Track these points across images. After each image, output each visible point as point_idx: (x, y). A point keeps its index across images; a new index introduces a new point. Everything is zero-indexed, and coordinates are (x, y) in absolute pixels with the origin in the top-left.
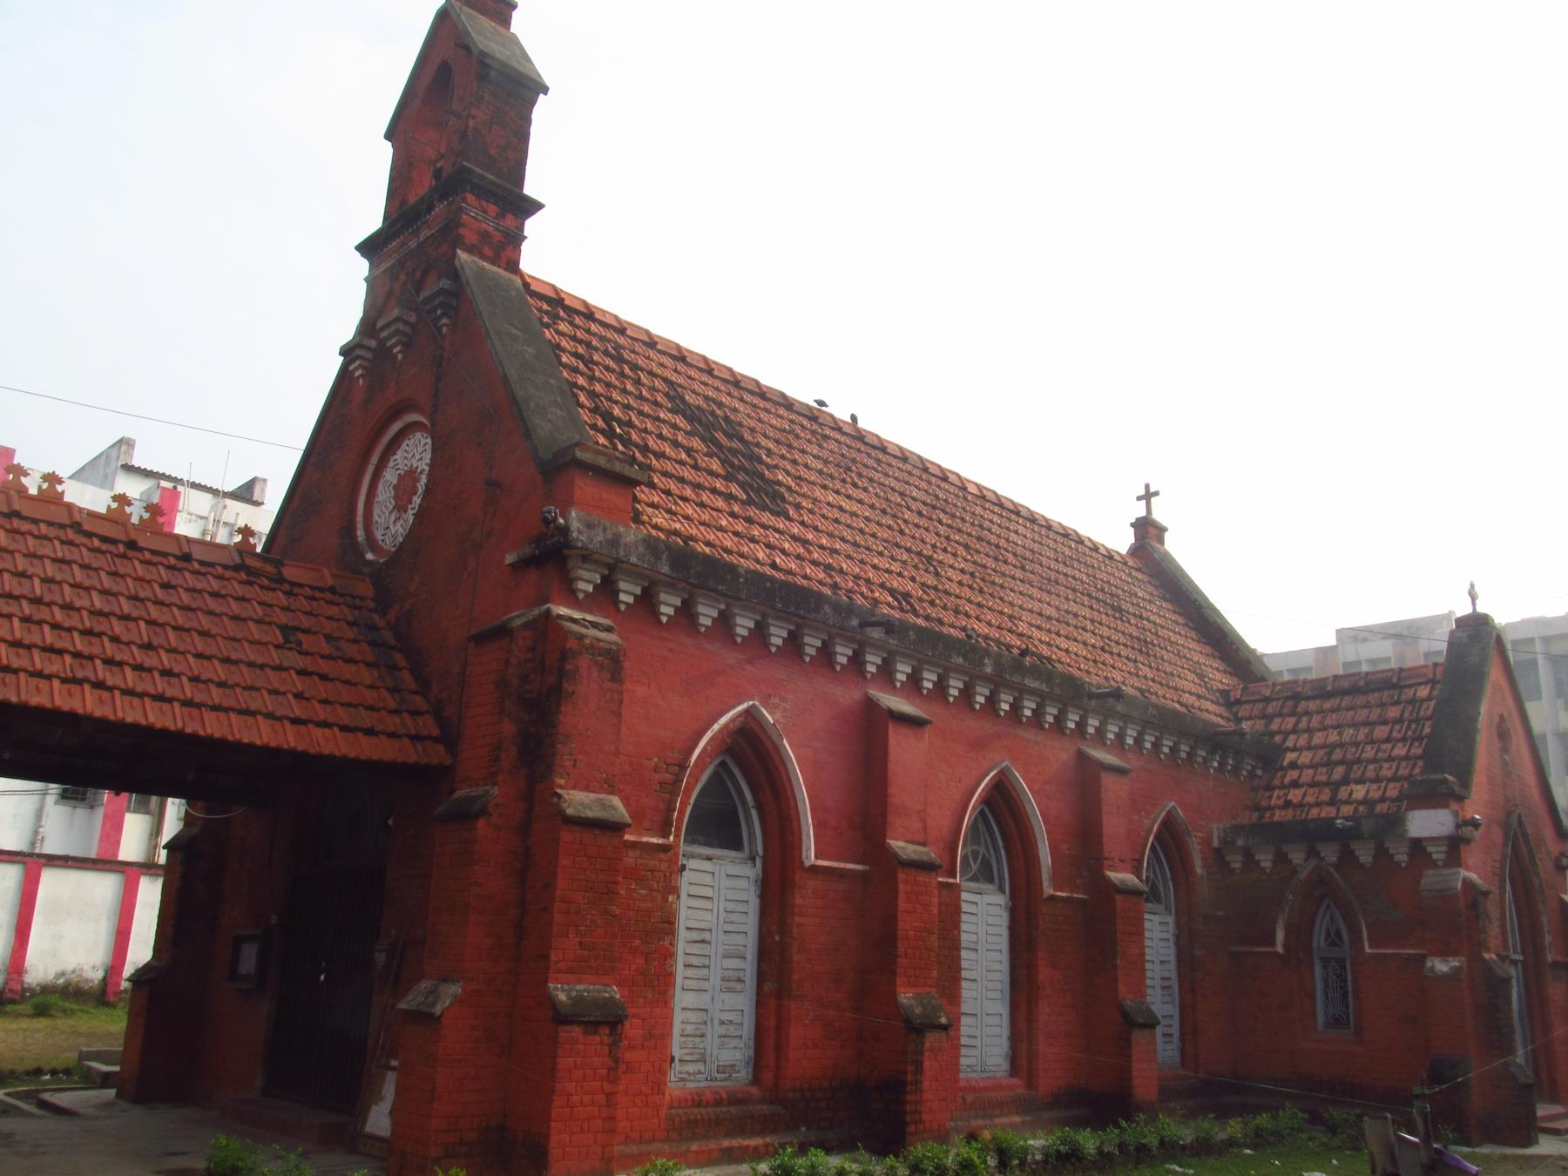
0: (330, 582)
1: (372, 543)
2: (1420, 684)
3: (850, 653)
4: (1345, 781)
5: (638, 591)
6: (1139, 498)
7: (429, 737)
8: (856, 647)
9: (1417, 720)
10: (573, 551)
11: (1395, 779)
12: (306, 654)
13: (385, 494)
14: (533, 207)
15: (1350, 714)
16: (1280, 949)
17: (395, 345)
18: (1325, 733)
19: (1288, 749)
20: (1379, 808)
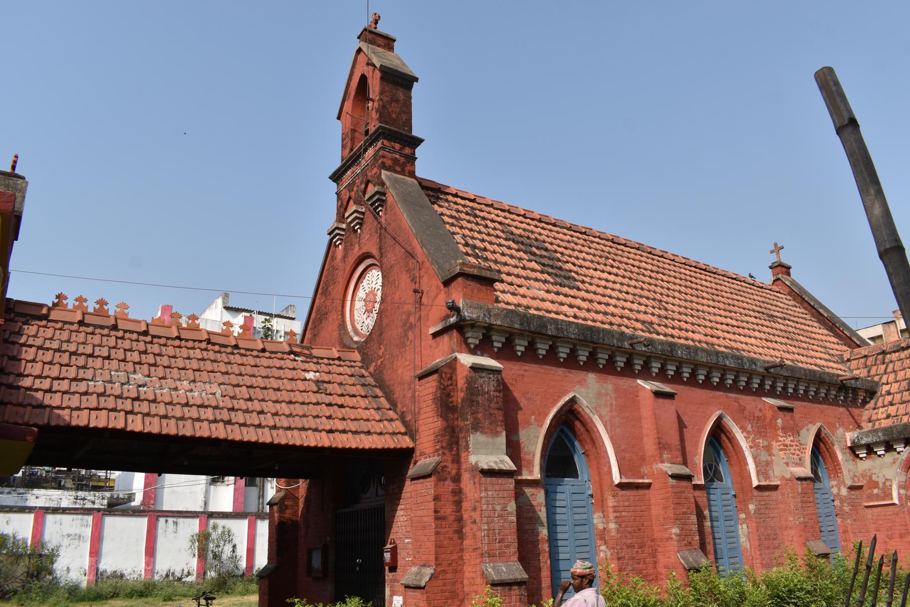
0: (337, 355)
1: (356, 332)
3: (625, 360)
5: (503, 340)
6: (772, 252)
7: (400, 433)
12: (330, 394)
13: (359, 305)
14: (418, 142)
16: (896, 501)
17: (356, 225)
18: (904, 372)
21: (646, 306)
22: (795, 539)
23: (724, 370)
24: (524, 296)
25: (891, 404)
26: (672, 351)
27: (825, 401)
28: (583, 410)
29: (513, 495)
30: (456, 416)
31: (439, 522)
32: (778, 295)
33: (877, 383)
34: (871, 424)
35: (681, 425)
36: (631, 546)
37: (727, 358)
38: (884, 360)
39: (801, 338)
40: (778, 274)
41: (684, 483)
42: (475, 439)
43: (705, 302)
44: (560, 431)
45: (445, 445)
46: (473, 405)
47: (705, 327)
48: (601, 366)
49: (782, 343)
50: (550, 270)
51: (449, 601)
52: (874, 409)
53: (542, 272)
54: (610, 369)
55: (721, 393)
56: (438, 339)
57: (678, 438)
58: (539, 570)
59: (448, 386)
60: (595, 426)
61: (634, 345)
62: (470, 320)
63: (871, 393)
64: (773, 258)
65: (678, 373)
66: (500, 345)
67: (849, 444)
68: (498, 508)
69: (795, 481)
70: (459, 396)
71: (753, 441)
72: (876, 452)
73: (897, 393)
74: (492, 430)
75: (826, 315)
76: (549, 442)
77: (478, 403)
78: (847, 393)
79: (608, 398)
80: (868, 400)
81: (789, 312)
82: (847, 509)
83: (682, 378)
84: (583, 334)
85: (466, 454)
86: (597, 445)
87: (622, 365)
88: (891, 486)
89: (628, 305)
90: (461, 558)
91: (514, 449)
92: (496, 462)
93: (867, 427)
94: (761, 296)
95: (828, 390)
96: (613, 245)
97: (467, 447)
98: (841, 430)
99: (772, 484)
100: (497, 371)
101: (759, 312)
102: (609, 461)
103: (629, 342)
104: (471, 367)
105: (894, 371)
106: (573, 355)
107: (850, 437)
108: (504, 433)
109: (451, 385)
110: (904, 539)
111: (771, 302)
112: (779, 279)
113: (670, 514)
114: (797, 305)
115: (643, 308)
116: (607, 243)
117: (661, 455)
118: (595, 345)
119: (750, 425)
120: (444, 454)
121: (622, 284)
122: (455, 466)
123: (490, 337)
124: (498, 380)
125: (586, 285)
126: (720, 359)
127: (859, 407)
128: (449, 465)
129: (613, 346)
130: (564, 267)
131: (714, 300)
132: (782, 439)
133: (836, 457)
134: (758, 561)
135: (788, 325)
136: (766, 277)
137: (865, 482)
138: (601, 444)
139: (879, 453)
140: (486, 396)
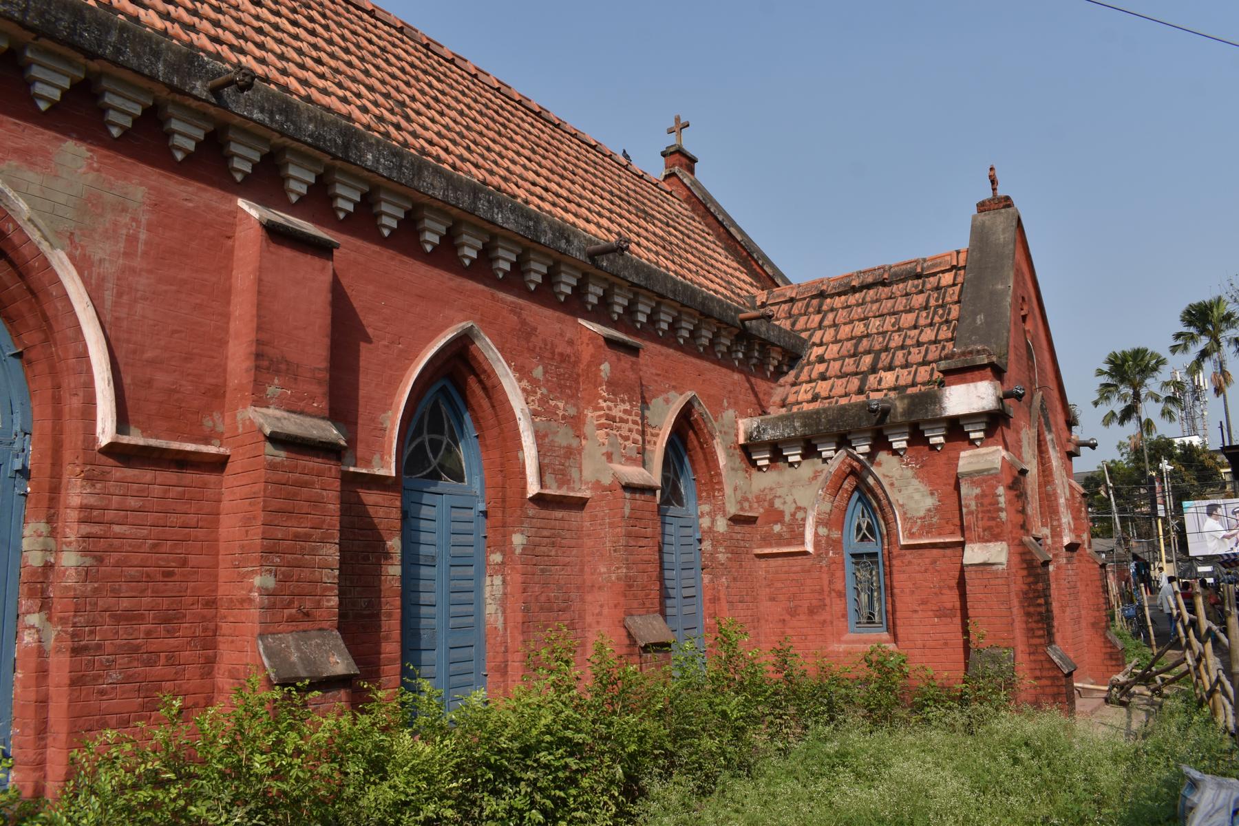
2: (943, 272)
4: (874, 369)
6: (670, 131)
9: (942, 306)
11: (924, 363)
15: (875, 306)
16: (809, 548)
18: (850, 326)
19: (814, 344)
22: (606, 611)
25: (823, 377)
26: (346, 147)
27: (708, 354)
28: (18, 228)
32: (668, 196)
33: (804, 342)
36: (131, 617)
38: (820, 306)
40: (674, 165)
52: (794, 384)
55: (481, 287)
60: (57, 281)
63: (792, 356)
64: (672, 140)
67: (742, 441)
69: (620, 491)
71: (543, 401)
72: (786, 457)
73: (834, 360)
75: (739, 238)
78: (749, 349)
79: (125, 219)
80: (785, 368)
82: (722, 557)
88: (804, 519)
93: (775, 412)
98: (730, 414)
99: (572, 494)
105: (835, 325)
107: (745, 426)
110: (816, 617)
114: (697, 218)
119: (540, 368)
127: (768, 380)
132: (604, 405)
133: (716, 461)
134: (518, 657)
136: (656, 169)
137: (761, 510)
138: (70, 333)
139: (791, 459)
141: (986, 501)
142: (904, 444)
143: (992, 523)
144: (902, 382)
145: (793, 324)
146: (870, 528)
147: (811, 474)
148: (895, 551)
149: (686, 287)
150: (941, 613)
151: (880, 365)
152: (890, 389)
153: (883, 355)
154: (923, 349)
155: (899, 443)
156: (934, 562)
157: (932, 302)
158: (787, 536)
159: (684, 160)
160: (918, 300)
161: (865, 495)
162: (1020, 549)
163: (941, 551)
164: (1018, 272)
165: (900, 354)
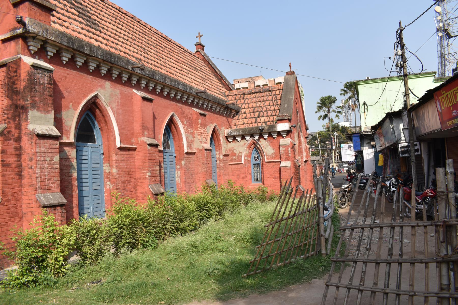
2: (276, 90)
3: (127, 77)
4: (259, 117)
5: (55, 51)
6: (197, 37)
8: (129, 75)
10: (30, 35)
15: (259, 98)
16: (243, 162)
18: (252, 104)
19: (243, 108)
20: (268, 124)
21: (138, 50)
22: (201, 178)
23: (177, 90)
24: (67, 28)
25: (246, 118)
26: (153, 76)
27: (218, 113)
28: (101, 102)
29: (58, 151)
30: (19, 98)
31: (5, 168)
32: (198, 59)
33: (240, 108)
34: (235, 126)
35: (154, 118)
36: (123, 182)
37: (180, 84)
38: (244, 97)
39: (208, 81)
40: (198, 49)
41: (154, 149)
42: (32, 113)
43: (166, 54)
44: (86, 114)
45: (10, 116)
46: (32, 91)
47: (167, 67)
48: (114, 78)
49: (200, 83)
50: (84, 17)
51: (12, 219)
52: (238, 120)
53: (79, 16)
54: (118, 80)
55: (174, 103)
56: (6, 44)
57: (153, 124)
58: (72, 196)
59: (13, 76)
60: (108, 113)
61: (134, 69)
62: (33, 33)
63: (237, 112)
64: (197, 40)
65: (155, 89)
66: (52, 55)
67: (226, 135)
68: (48, 159)
70: (22, 85)
71: (187, 129)
72: (237, 139)
74: (45, 109)
75: (218, 73)
76: (80, 120)
77: (36, 90)
78: (228, 111)
79: (116, 98)
80: (235, 115)
81: (203, 68)
82: (222, 165)
83: (156, 92)
84: (106, 57)
85: (26, 123)
86: (108, 125)
87: (126, 79)
89: (128, 47)
90: (21, 191)
91: (58, 123)
92: (47, 130)
93: (234, 128)
94: (191, 58)
95: (220, 108)
96: (119, 12)
97: (27, 119)
98: (223, 128)
99: (193, 151)
100: (51, 71)
101: (190, 65)
102: (115, 135)
103: (132, 66)
104: (31, 65)
105: (248, 103)
106: (98, 69)
108: (53, 112)
109: (16, 76)
110: (244, 180)
111: (195, 61)
112: (199, 51)
113: (146, 164)
114: (206, 66)
115: (136, 50)
116: (116, 10)
117: (143, 132)
118: (112, 65)
120: (9, 122)
121: (124, 35)
122: (17, 131)
123: (46, 48)
124: (50, 77)
125: (105, 30)
126: (177, 84)
128: (13, 130)
129: (122, 67)
130: (91, 17)
131: (170, 55)
132: (200, 130)
133: (220, 141)
134: (184, 189)
135: (202, 75)
136: (193, 50)
138: (111, 124)
139: (238, 140)
140: (42, 86)
141: (286, 151)
142: (267, 137)
143: (287, 157)
144: (266, 121)
145: (237, 102)
146: (258, 157)
147: (243, 144)
148: (264, 163)
149: (215, 97)
150: (275, 178)
151: (260, 116)
152: (263, 122)
153: (261, 113)
154: (271, 112)
155: (266, 136)
156: (273, 166)
157: (274, 99)
158: (237, 159)
159: (202, 47)
160: (270, 98)
161: (256, 149)
162: (294, 163)
163: (275, 163)
164: (295, 92)
165: (265, 113)
